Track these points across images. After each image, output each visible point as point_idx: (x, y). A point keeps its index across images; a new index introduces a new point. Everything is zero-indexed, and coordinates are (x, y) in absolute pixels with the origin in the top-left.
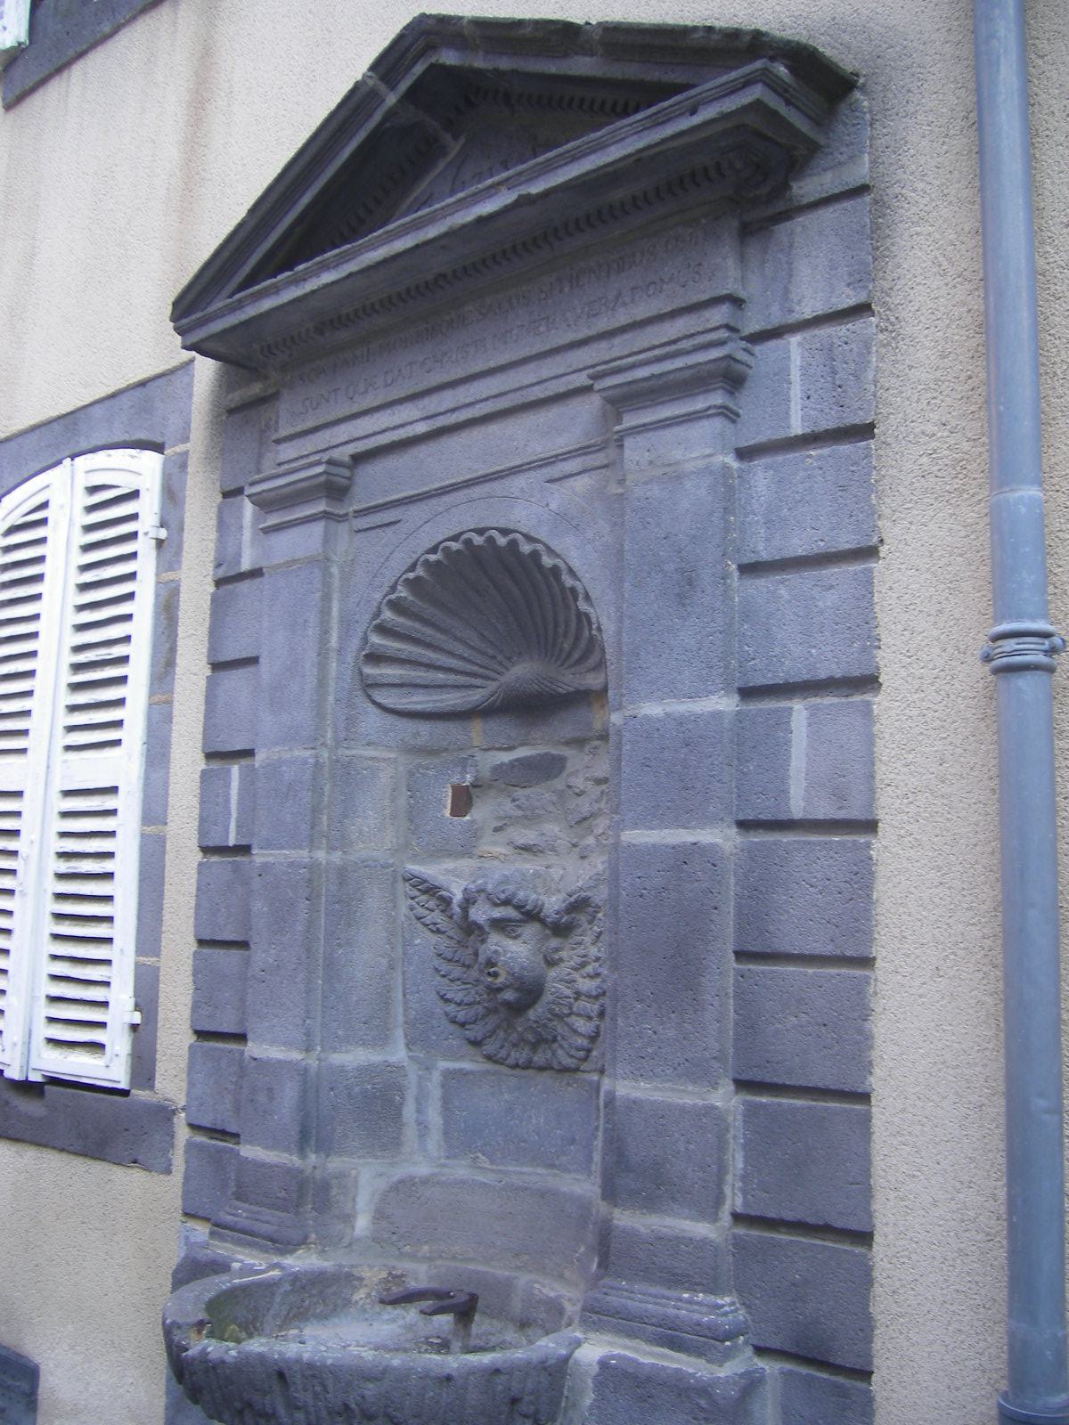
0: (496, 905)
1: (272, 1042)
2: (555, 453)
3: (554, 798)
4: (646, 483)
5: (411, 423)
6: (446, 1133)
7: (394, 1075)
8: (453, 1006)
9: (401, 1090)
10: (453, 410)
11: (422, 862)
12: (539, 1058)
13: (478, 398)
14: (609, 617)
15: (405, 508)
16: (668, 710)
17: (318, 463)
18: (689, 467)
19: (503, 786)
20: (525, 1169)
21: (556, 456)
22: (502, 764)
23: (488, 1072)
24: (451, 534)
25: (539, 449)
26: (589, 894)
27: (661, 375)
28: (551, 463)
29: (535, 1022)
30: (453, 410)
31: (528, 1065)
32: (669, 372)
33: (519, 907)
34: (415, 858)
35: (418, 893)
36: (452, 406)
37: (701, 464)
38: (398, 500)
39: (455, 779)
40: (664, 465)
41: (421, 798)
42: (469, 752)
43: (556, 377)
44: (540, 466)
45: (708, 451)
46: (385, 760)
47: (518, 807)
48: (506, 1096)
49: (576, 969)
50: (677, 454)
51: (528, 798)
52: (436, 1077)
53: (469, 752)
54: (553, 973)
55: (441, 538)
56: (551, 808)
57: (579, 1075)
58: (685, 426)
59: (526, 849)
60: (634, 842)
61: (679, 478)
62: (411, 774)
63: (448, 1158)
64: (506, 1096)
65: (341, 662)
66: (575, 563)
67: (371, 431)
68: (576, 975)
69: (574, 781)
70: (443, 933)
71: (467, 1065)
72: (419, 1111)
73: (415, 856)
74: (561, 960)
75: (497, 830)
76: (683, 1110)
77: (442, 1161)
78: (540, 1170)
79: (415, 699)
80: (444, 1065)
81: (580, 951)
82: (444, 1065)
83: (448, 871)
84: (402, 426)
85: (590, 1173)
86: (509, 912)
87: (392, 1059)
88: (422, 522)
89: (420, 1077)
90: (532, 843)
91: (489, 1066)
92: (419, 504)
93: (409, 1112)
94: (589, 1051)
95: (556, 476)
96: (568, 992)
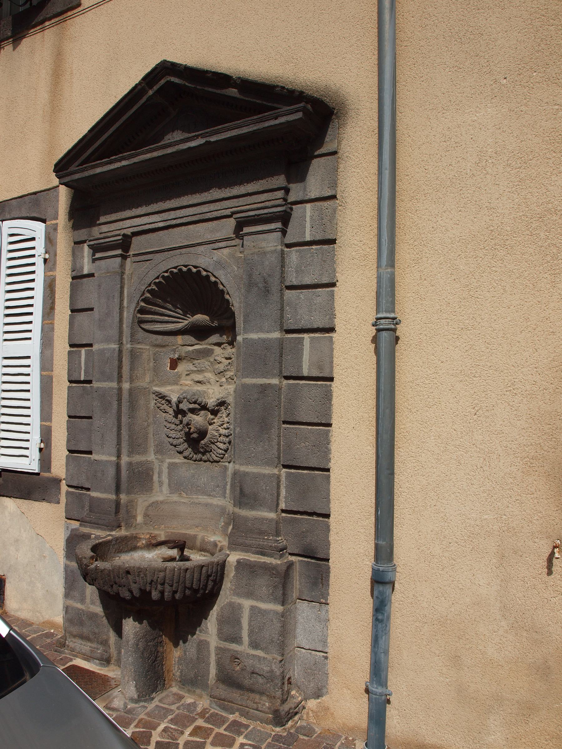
0: (191, 403)
1: (103, 454)
2: (215, 239)
3: (209, 364)
4: (252, 254)
5: (157, 222)
6: (169, 485)
7: (149, 465)
8: (172, 439)
9: (152, 469)
10: (175, 219)
11: (159, 386)
12: (204, 458)
13: (185, 215)
14: (237, 302)
15: (154, 255)
16: (259, 336)
17: (119, 235)
18: (268, 249)
19: (189, 359)
20: (199, 497)
21: (216, 240)
22: (189, 351)
23: (185, 463)
24: (173, 266)
25: (209, 237)
26: (226, 399)
27: (259, 215)
28: (214, 243)
29: (204, 445)
30: (175, 219)
31: (201, 460)
32: (262, 214)
33: (199, 404)
34: (156, 385)
35: (158, 398)
36: (174, 217)
37: (273, 248)
38: (151, 252)
39: (171, 356)
40: (259, 248)
41: (159, 363)
42: (177, 346)
43: (216, 211)
44: (210, 244)
45: (275, 244)
46: (145, 349)
47: (196, 367)
48: (192, 471)
49: (220, 426)
50: (264, 244)
51: (199, 364)
52: (165, 465)
53: (177, 346)
54: (210, 427)
55: (169, 268)
56: (208, 367)
57: (220, 463)
58: (267, 234)
59: (199, 382)
60: (247, 383)
61: (265, 253)
62: (155, 354)
63: (170, 494)
64: (192, 471)
65: (128, 312)
66: (223, 281)
67: (140, 224)
68: (220, 428)
69: (217, 358)
70: (168, 413)
71: (177, 461)
72: (159, 477)
73: (157, 384)
74: (214, 423)
75: (187, 375)
76: (264, 475)
77: (168, 495)
78: (205, 497)
79: (156, 326)
80: (168, 461)
81: (221, 419)
82: (168, 461)
83: (169, 390)
84: (154, 223)
85: (225, 497)
86: (197, 406)
87: (149, 459)
88: (161, 261)
89: (159, 465)
90: (201, 380)
91: (186, 461)
92: (160, 253)
93: (155, 478)
94: (224, 455)
95: (216, 248)
96: (216, 434)
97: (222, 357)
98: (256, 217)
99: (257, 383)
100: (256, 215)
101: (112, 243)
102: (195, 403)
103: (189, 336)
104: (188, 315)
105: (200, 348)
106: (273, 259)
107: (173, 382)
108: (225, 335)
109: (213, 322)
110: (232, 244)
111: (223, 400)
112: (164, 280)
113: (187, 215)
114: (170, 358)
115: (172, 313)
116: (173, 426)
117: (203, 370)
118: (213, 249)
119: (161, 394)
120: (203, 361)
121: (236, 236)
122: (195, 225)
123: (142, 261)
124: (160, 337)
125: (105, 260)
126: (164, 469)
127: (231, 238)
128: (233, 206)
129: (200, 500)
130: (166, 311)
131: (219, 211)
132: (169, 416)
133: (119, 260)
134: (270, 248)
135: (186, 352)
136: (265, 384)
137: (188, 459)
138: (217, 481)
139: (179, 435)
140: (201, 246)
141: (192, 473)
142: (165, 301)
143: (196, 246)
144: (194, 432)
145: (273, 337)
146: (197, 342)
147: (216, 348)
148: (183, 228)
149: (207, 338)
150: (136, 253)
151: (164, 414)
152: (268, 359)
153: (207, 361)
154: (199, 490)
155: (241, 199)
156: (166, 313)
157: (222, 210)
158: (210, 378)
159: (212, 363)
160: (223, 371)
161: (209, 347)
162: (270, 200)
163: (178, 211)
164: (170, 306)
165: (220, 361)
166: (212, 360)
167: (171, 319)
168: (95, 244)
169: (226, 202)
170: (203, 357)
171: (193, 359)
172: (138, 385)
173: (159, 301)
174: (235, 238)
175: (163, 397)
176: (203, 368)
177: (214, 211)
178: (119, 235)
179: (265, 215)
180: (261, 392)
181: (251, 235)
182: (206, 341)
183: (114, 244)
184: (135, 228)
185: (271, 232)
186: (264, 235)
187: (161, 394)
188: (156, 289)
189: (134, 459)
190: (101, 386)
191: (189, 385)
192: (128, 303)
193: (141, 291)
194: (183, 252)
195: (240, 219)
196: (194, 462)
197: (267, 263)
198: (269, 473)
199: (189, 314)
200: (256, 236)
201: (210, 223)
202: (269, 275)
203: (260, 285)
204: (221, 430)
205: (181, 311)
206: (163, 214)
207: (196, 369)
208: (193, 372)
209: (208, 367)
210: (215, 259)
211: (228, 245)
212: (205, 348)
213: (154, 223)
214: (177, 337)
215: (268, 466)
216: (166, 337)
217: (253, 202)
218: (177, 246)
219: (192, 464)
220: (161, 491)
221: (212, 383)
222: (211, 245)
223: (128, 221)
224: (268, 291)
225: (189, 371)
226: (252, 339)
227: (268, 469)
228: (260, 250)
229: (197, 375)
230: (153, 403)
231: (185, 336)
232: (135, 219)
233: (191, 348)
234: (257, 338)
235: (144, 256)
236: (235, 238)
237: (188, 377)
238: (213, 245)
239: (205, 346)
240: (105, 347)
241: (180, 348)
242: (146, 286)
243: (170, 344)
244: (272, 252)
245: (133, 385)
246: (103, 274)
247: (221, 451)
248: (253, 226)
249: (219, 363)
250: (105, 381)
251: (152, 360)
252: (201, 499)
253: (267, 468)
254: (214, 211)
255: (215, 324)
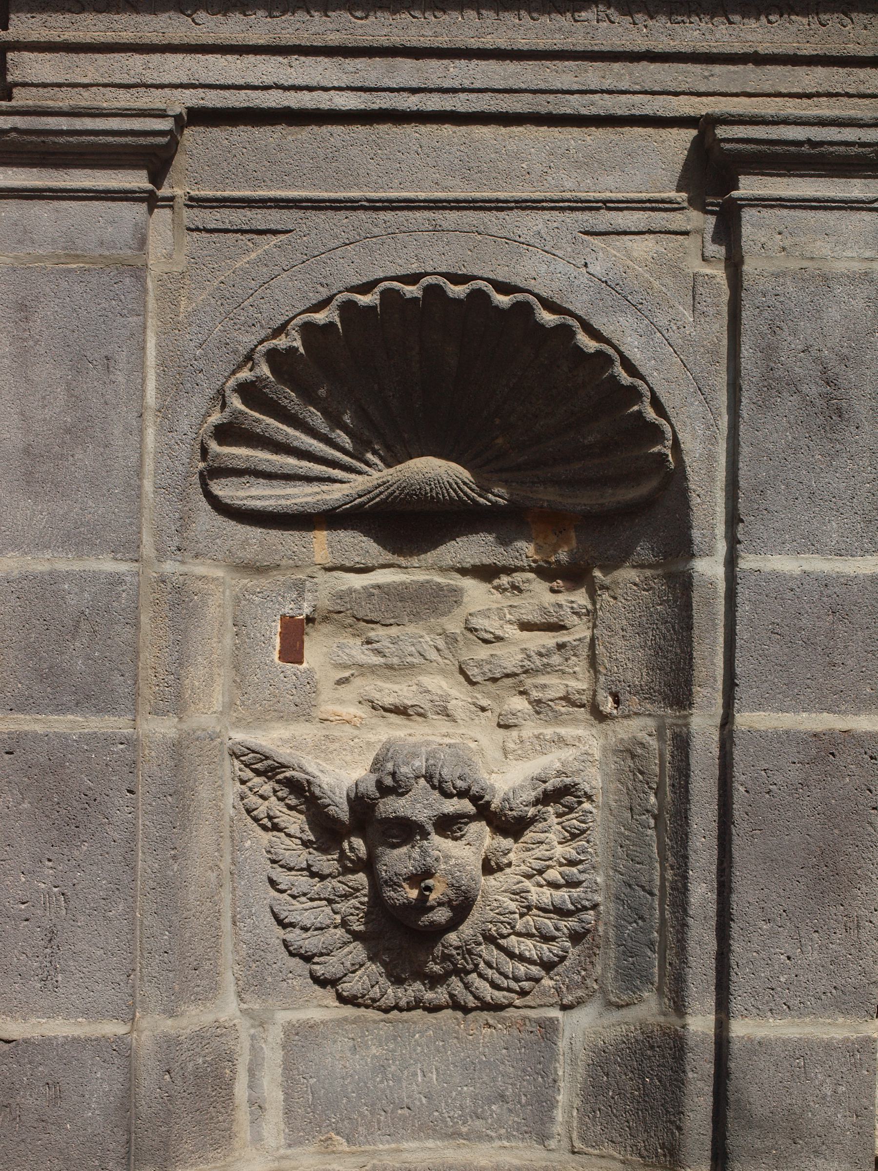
0: (448, 795)
1: (52, 1012)
2: (598, 196)
3: (441, 643)
4: (776, 276)
5: (326, 89)
6: (288, 1112)
7: (223, 1039)
8: (297, 931)
9: (230, 1058)
10: (414, 91)
11: (248, 726)
12: (440, 995)
13: (467, 84)
14: (694, 437)
15: (301, 213)
16: (806, 567)
17: (161, 114)
18: (841, 267)
19: (350, 621)
20: (405, 1145)
21: (605, 202)
22: (351, 591)
23: (345, 1019)
24: (401, 271)
25: (569, 184)
26: (577, 780)
27: (821, 143)
28: (591, 209)
29: (457, 948)
30: (414, 91)
31: (417, 1004)
32: (832, 143)
33: (476, 800)
34: (238, 723)
35: (251, 774)
36: (414, 84)
37: (857, 267)
38: (288, 201)
39: (288, 609)
40: (803, 257)
41: (248, 634)
42: (308, 571)
43: (610, 92)
44: (572, 209)
45: (868, 254)
46: (213, 579)
47: (378, 652)
48: (374, 1050)
49: (529, 877)
50: (822, 247)
51: (394, 641)
52: (275, 1034)
53: (308, 571)
54: (492, 882)
55: (381, 275)
56: (433, 655)
57: (510, 1012)
58: (837, 213)
59: (401, 711)
60: (757, 726)
61: (826, 278)
62: (237, 600)
63: (290, 1146)
64: (374, 1050)
65: (167, 428)
66: (636, 355)
67: (241, 82)
68: (527, 884)
69: (478, 622)
70: (280, 830)
71: (314, 1014)
72: (251, 1087)
73: (239, 720)
74: (509, 865)
75: (341, 682)
76: (828, 1047)
77: (282, 1151)
78: (430, 1144)
79: (254, 492)
80: (283, 1017)
81: (541, 851)
82: (283, 1017)
83: (285, 741)
84: (310, 89)
85: (543, 1138)
86: (466, 806)
87: (223, 1017)
88: (338, 243)
89: (253, 1037)
90: (409, 703)
91: (349, 1011)
92: (330, 213)
93: (241, 1090)
94: (537, 980)
95: (602, 228)
96: (513, 906)
97: (510, 622)
98: (805, 149)
99: (802, 728)
100: (809, 141)
101: (110, 139)
102: (462, 794)
103: (357, 534)
104: (369, 456)
105: (402, 583)
106: (859, 304)
107: (294, 708)
108: (529, 540)
109: (484, 490)
110: (673, 227)
111: (568, 780)
112: (341, 322)
113: (477, 85)
114: (283, 616)
115: (314, 442)
116: (303, 882)
117: (412, 666)
118: (586, 233)
119: (267, 758)
120: (411, 629)
121: (690, 201)
122: (503, 130)
123: (236, 231)
124: (255, 533)
125: (56, 204)
126: (267, 1052)
127: (671, 202)
128: (684, 87)
129: (405, 1156)
130: (297, 433)
131: (623, 98)
132: (287, 841)
133: (136, 211)
134: (847, 264)
135: (340, 596)
136: (831, 732)
137: (358, 1005)
138: (494, 1080)
139: (323, 914)
140: (533, 214)
141: (374, 1057)
142: (308, 396)
143: (511, 209)
144: (440, 904)
145: (859, 571)
146: (388, 557)
147: (469, 584)
148: (448, 130)
149: (435, 545)
150: (204, 193)
151: (266, 837)
152: (841, 645)
153: (431, 630)
154: (403, 1119)
155: (718, 69)
156: (296, 444)
157: (634, 93)
158: (446, 698)
159: (452, 640)
160: (518, 670)
161: (439, 579)
162: (837, 95)
163: (434, 63)
164: (316, 418)
165: (499, 633)
166: (454, 626)
167: (291, 463)
168: (15, 129)
169: (653, 67)
170: (416, 616)
171: (368, 622)
172: (195, 725)
173: (290, 398)
174: (685, 204)
175: (272, 769)
176: (410, 659)
177: (602, 92)
178: (161, 114)
179: (842, 149)
180: (813, 762)
181: (772, 207)
182: (430, 557)
183: (126, 145)
184: (212, 94)
185: (852, 209)
186: (821, 214)
187: (267, 758)
188: (302, 350)
189: (184, 1022)
190: (39, 728)
191: (357, 722)
192: (162, 392)
193: (235, 352)
194: (445, 225)
195: (741, 146)
196: (383, 1016)
197: (833, 313)
198: (847, 1039)
199: (375, 453)
200: (792, 212)
201: (575, 131)
202: (844, 359)
203: (812, 390)
204: (533, 889)
205: (347, 440)
206: (360, 63)
207: (377, 660)
208: (364, 669)
209: (433, 655)
210: (596, 268)
211: (654, 226)
212: (422, 584)
213: (310, 89)
214: (311, 534)
215: (846, 1012)
216: (274, 535)
217: (767, 88)
218: (422, 195)
219: (375, 1022)
220: (257, 1139)
221: (459, 714)
222: (578, 215)
223: (177, 59)
224: (839, 412)
225: (346, 667)
226: (776, 575)
227: (843, 1026)
228: (805, 264)
229: (380, 683)
230: (233, 790)
231: (342, 534)
232: (211, 58)
233: (357, 581)
234: (797, 571)
235: (248, 213)
236: (685, 204)
237: (343, 690)
238: (587, 215)
239: (421, 576)
240: (62, 566)
241: (322, 577)
242: (263, 334)
243: (284, 562)
244: (853, 279)
245: (184, 726)
246: (40, 258)
247: (522, 969)
248: (811, 176)
249: (486, 641)
250: (60, 709)
251: (230, 623)
252: (413, 1151)
253: (841, 1020)
254: (602, 92)
255: (499, 495)
